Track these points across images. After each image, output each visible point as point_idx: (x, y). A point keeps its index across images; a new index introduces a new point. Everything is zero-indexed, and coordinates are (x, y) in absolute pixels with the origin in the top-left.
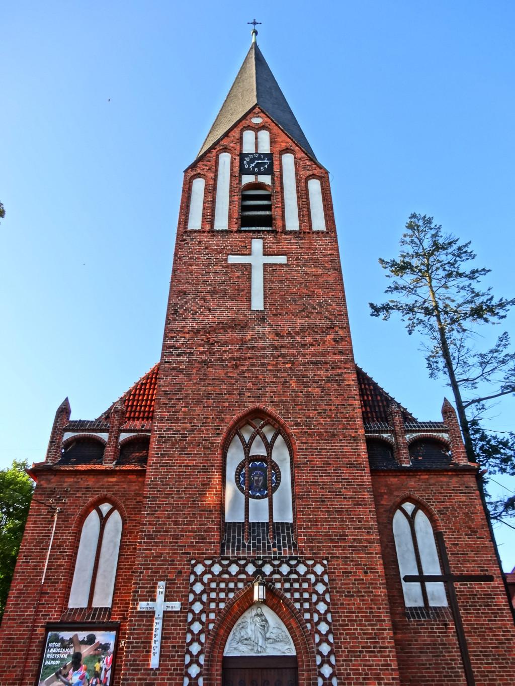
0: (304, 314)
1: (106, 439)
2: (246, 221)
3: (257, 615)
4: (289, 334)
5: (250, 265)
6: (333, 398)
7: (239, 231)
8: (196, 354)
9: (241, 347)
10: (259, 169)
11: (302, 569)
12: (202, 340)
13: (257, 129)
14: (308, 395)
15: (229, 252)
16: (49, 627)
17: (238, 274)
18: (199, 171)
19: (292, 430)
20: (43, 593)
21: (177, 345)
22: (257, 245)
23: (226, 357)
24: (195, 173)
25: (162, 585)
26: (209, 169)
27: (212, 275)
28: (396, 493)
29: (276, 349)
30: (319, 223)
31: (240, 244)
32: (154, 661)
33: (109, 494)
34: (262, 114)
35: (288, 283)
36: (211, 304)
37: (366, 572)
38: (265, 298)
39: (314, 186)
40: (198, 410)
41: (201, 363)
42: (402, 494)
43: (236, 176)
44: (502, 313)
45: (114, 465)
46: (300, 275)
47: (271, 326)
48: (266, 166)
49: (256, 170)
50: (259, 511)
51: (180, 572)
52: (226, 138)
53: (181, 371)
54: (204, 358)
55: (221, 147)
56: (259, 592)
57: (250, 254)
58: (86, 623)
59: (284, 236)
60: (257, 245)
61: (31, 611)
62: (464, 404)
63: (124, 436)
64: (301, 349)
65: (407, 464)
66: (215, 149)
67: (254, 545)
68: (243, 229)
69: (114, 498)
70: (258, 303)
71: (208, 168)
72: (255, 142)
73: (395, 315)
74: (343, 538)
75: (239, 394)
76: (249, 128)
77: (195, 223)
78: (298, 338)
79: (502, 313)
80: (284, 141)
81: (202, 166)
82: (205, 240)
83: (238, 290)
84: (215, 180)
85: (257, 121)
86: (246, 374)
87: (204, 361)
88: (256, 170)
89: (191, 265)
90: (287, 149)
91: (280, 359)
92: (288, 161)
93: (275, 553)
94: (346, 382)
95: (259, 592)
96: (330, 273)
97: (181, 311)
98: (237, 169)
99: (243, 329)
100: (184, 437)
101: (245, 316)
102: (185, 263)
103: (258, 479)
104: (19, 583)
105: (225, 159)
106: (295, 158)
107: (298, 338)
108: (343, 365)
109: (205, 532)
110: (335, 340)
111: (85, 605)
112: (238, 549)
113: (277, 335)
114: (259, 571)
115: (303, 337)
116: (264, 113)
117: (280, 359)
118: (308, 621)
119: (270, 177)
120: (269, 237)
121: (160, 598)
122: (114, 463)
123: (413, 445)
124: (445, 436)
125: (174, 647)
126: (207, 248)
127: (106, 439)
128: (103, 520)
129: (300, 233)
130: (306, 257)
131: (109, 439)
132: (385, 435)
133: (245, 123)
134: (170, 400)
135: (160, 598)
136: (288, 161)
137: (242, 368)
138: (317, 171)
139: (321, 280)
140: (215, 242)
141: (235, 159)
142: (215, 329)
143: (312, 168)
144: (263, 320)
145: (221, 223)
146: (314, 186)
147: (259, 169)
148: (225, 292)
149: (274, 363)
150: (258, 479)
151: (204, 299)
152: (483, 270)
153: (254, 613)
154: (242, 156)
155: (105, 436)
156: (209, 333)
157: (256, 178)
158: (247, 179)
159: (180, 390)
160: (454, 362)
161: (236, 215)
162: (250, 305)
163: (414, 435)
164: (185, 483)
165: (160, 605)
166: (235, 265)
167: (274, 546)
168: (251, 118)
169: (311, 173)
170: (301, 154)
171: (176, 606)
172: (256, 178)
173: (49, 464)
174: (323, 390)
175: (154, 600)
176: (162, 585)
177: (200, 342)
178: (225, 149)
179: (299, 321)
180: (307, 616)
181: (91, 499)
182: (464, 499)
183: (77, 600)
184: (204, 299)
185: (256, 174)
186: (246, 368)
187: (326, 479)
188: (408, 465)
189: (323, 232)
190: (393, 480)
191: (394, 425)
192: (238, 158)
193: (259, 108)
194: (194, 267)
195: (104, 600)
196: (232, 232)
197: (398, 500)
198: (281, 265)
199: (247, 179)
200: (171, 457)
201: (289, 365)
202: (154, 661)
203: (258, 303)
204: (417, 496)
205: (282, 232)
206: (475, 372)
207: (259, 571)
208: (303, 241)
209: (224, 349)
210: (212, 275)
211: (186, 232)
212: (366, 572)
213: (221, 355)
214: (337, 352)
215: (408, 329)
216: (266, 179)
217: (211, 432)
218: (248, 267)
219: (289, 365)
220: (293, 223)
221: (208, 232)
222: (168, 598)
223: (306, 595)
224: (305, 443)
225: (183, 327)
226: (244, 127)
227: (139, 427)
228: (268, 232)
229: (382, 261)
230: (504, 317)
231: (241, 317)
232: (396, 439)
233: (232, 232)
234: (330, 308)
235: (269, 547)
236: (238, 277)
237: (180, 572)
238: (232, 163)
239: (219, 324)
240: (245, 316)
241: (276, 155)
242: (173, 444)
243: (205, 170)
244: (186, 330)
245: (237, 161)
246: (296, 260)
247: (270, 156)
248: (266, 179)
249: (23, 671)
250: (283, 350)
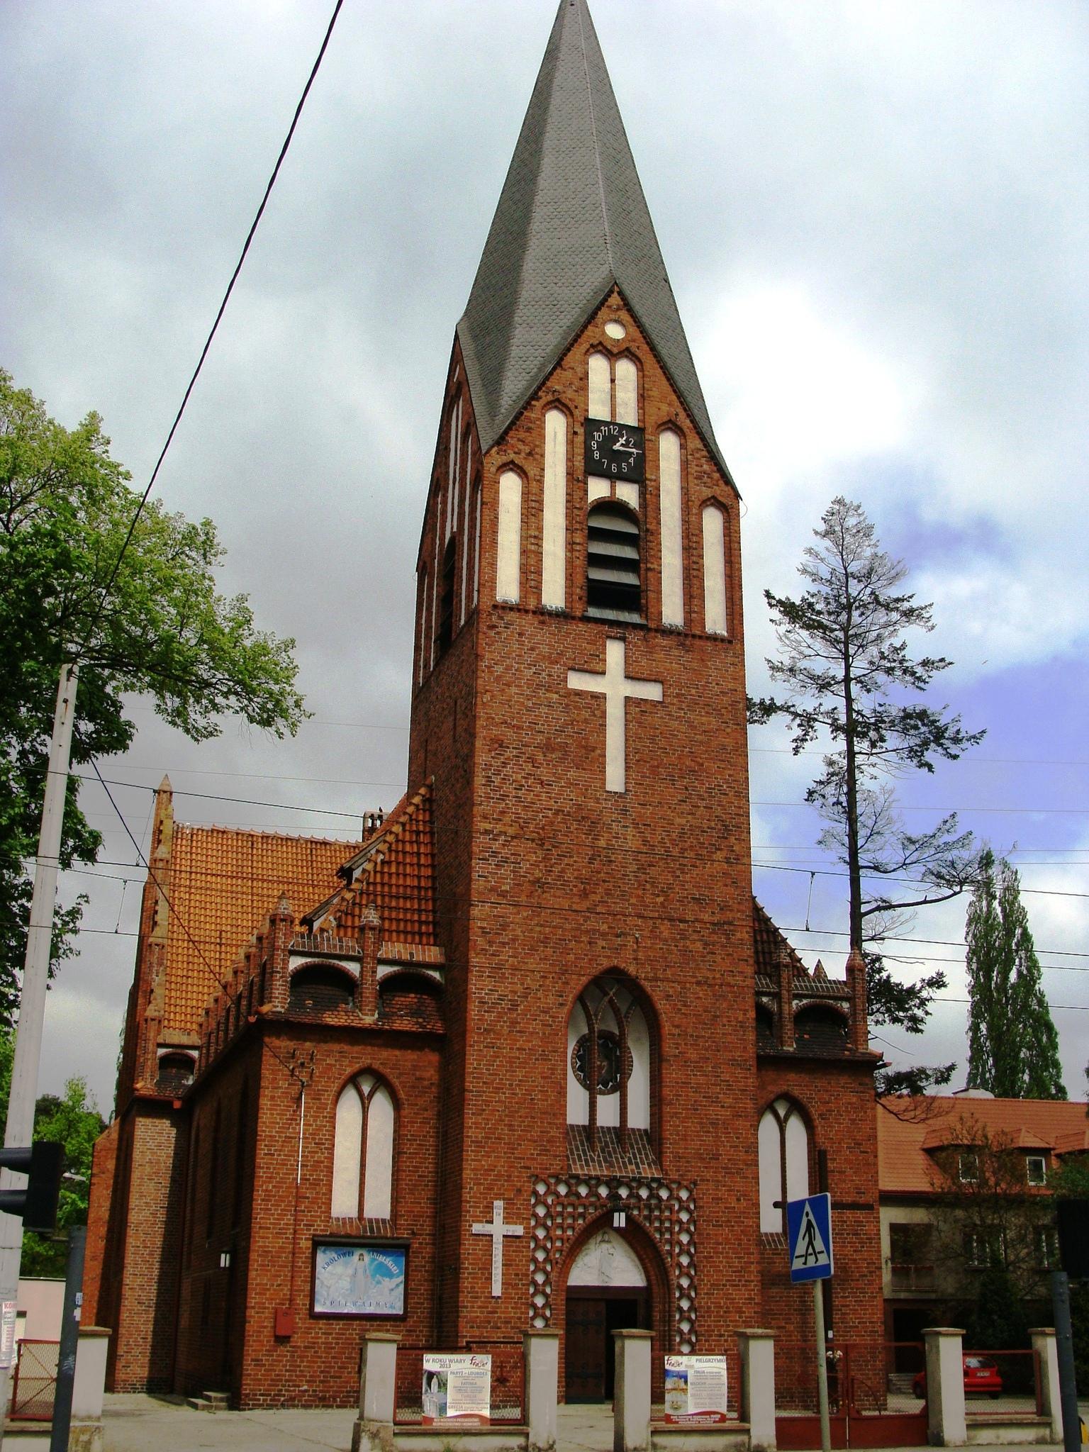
0: (686, 807)
1: (357, 974)
2: (599, 594)
3: (603, 1241)
4: (662, 842)
5: (604, 696)
6: (718, 958)
8: (525, 866)
9: (592, 859)
10: (619, 467)
11: (664, 1194)
12: (533, 840)
13: (613, 354)
14: (685, 952)
15: (570, 663)
16: (319, 1243)
17: (585, 714)
18: (512, 456)
19: (661, 1005)
20: (299, 1197)
21: (496, 846)
22: (615, 653)
23: (569, 875)
24: (505, 459)
25: (499, 1204)
26: (530, 454)
28: (769, 1088)
29: (642, 869)
30: (715, 620)
31: (588, 647)
32: (497, 1290)
33: (376, 1065)
34: (624, 315)
35: (663, 743)
36: (544, 773)
37: (738, 1200)
38: (627, 768)
39: (712, 521)
40: (532, 963)
41: (533, 883)
43: (578, 481)
44: (954, 750)
45: (378, 1020)
46: (683, 729)
47: (636, 825)
48: (632, 460)
49: (614, 468)
50: (607, 1113)
51: (519, 1191)
52: (558, 371)
53: (503, 894)
54: (538, 874)
55: (550, 398)
56: (620, 1220)
57: (603, 673)
58: (364, 1237)
59: (661, 641)
60: (615, 653)
61: (289, 1218)
62: (864, 908)
63: (383, 971)
64: (678, 873)
65: (790, 1048)
66: (538, 399)
67: (606, 1161)
68: (593, 612)
69: (381, 1069)
70: (615, 778)
71: (527, 449)
72: (611, 390)
73: (779, 719)
74: (716, 1157)
75: (590, 943)
77: (508, 587)
78: (675, 852)
79: (954, 750)
80: (665, 408)
82: (529, 630)
83: (585, 747)
84: (540, 481)
85: (615, 332)
86: (599, 909)
87: (538, 880)
88: (614, 468)
89: (508, 685)
90: (670, 421)
91: (648, 886)
92: (668, 446)
93: (633, 1171)
94: (739, 935)
95: (620, 1220)
96: (729, 730)
97: (497, 780)
98: (579, 463)
99: (592, 824)
100: (515, 1006)
101: (597, 800)
102: (498, 678)
103: (603, 1068)
104: (264, 1182)
105: (555, 424)
106: (682, 447)
107: (675, 852)
108: (736, 906)
109: (548, 1141)
110: (727, 860)
111: (354, 1214)
112: (588, 1165)
113: (645, 841)
114: (614, 1196)
115: (683, 850)
116: (630, 311)
117: (648, 886)
118: (670, 1253)
119: (636, 487)
120: (633, 637)
122: (376, 1016)
123: (802, 1016)
124: (846, 1005)
125: (517, 1275)
126: (532, 649)
127: (357, 974)
128: (365, 1103)
129: (686, 635)
130: (693, 691)
131: (361, 972)
134: (491, 943)
136: (668, 446)
137: (592, 897)
138: (720, 491)
139: (714, 744)
140: (545, 638)
141: (575, 433)
142: (552, 823)
143: (714, 487)
144: (624, 811)
145: (554, 594)
146: (712, 521)
147: (619, 467)
148: (564, 748)
149: (640, 892)
150: (603, 1068)
151: (532, 760)
152: (942, 660)
153: (599, 1238)
154: (591, 425)
155: (353, 968)
156: (543, 829)
157: (613, 488)
158: (598, 489)
159: (504, 927)
160: (862, 833)
161: (579, 580)
162: (604, 780)
163: (805, 1001)
164: (520, 1074)
165: (499, 1228)
166: (579, 693)
167: (631, 1163)
168: (604, 323)
169: (707, 493)
170: (694, 443)
171: (519, 1230)
172: (613, 488)
173: (279, 1009)
174: (706, 944)
175: (492, 1222)
176: (499, 1204)
177: (530, 844)
178: (558, 404)
179: (678, 820)
180: (667, 1247)
181: (349, 1071)
182: (854, 1100)
183: (343, 1204)
184: (532, 760)
185: (613, 478)
186: (598, 898)
187: (702, 1080)
188: (791, 1049)
189: (723, 640)
191: (780, 986)
192: (581, 430)
193: (620, 293)
194: (514, 690)
195: (379, 1206)
196: (573, 618)
197: (772, 1096)
198: (654, 704)
199: (598, 489)
200: (499, 1035)
201: (662, 899)
202: (497, 1290)
203: (615, 778)
204: (796, 1092)
205: (656, 631)
206: (890, 853)
207: (614, 1196)
208: (689, 656)
209: (566, 861)
210: (544, 710)
211: (495, 607)
212: (738, 1200)
213: (563, 871)
214: (729, 881)
215: (794, 745)
216: (628, 493)
217: (551, 999)
218: (600, 698)
219: (662, 899)
220: (672, 612)
221: (534, 613)
222: (508, 1220)
223: (667, 1224)
224: (677, 1027)
225: (503, 813)
226: (592, 346)
227: (406, 957)
228: (635, 626)
229: (768, 595)
230: (955, 757)
231: (592, 804)
232: (780, 1007)
233: (573, 618)
234: (724, 799)
235: (626, 1167)
236: (586, 721)
237: (519, 1191)
238: (570, 443)
239: (557, 812)
240: (597, 800)
241: (649, 430)
242: (500, 1015)
243: (523, 455)
244: (507, 819)
245: (580, 439)
246: (678, 695)
247: (637, 432)
248: (628, 493)
249: (291, 1290)
250: (652, 871)
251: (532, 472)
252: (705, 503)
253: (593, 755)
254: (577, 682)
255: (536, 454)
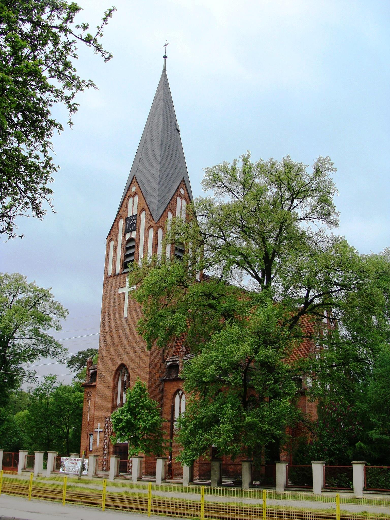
7: (123, 274)
25: (99, 424)
27: (113, 301)
36: (112, 317)
42: (177, 388)
76: (130, 196)
81: (112, 235)
84: (117, 241)
98: (124, 232)
105: (121, 222)
121: (99, 428)
132: (178, 362)
133: (128, 195)
135: (99, 428)
136: (143, 215)
145: (118, 271)
148: (116, 309)
151: (111, 315)
154: (127, 219)
158: (128, 236)
166: (120, 294)
169: (149, 225)
176: (99, 424)
190: (175, 383)
251: (115, 239)
252: (149, 228)
253: (122, 309)
254: (121, 291)
255: (117, 234)
